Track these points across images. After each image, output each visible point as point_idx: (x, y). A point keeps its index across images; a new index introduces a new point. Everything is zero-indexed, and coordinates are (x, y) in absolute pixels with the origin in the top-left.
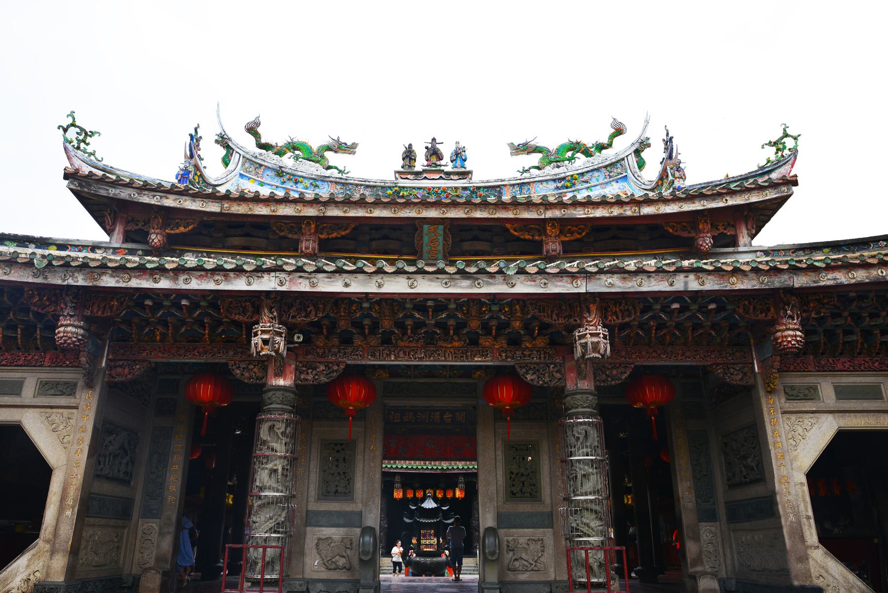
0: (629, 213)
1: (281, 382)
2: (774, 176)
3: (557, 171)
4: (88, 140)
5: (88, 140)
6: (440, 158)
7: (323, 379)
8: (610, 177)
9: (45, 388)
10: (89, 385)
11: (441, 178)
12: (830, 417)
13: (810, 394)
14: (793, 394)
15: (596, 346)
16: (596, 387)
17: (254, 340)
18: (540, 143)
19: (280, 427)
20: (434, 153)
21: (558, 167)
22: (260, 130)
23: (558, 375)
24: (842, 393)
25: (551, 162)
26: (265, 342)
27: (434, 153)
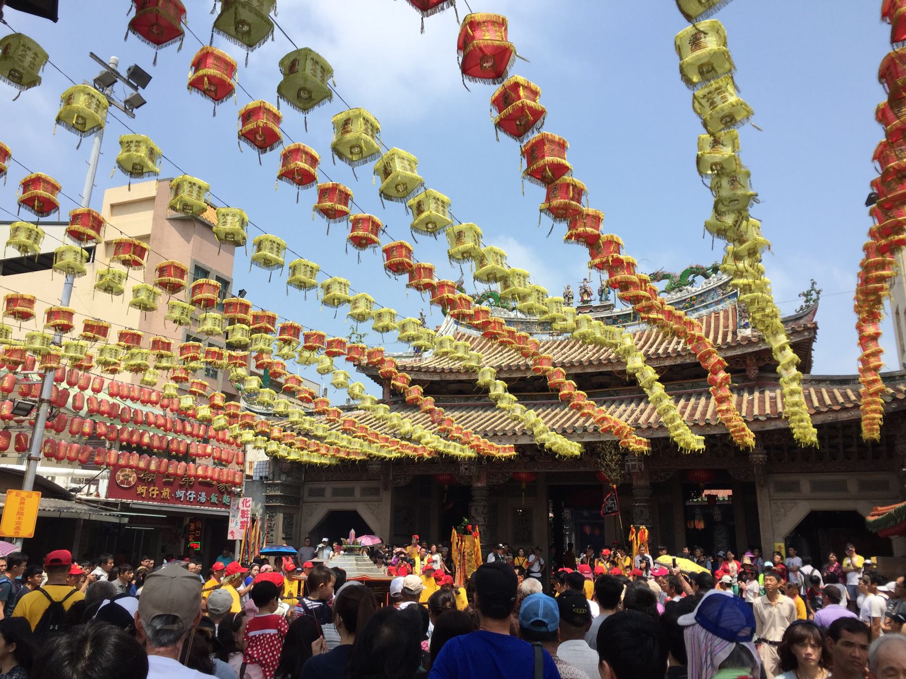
0: (688, 361)
1: (480, 485)
2: (802, 322)
3: (679, 295)
4: (363, 339)
5: (363, 339)
6: (589, 295)
7: (501, 482)
8: (724, 294)
9: (366, 491)
10: (386, 489)
11: (591, 311)
12: (805, 503)
13: (794, 487)
14: (782, 488)
15: (634, 466)
16: (651, 484)
17: (461, 468)
18: (667, 270)
19: (480, 509)
20: (585, 291)
21: (681, 291)
22: (463, 286)
23: (628, 477)
24: (815, 487)
25: (673, 289)
26: (466, 469)
27: (585, 291)
